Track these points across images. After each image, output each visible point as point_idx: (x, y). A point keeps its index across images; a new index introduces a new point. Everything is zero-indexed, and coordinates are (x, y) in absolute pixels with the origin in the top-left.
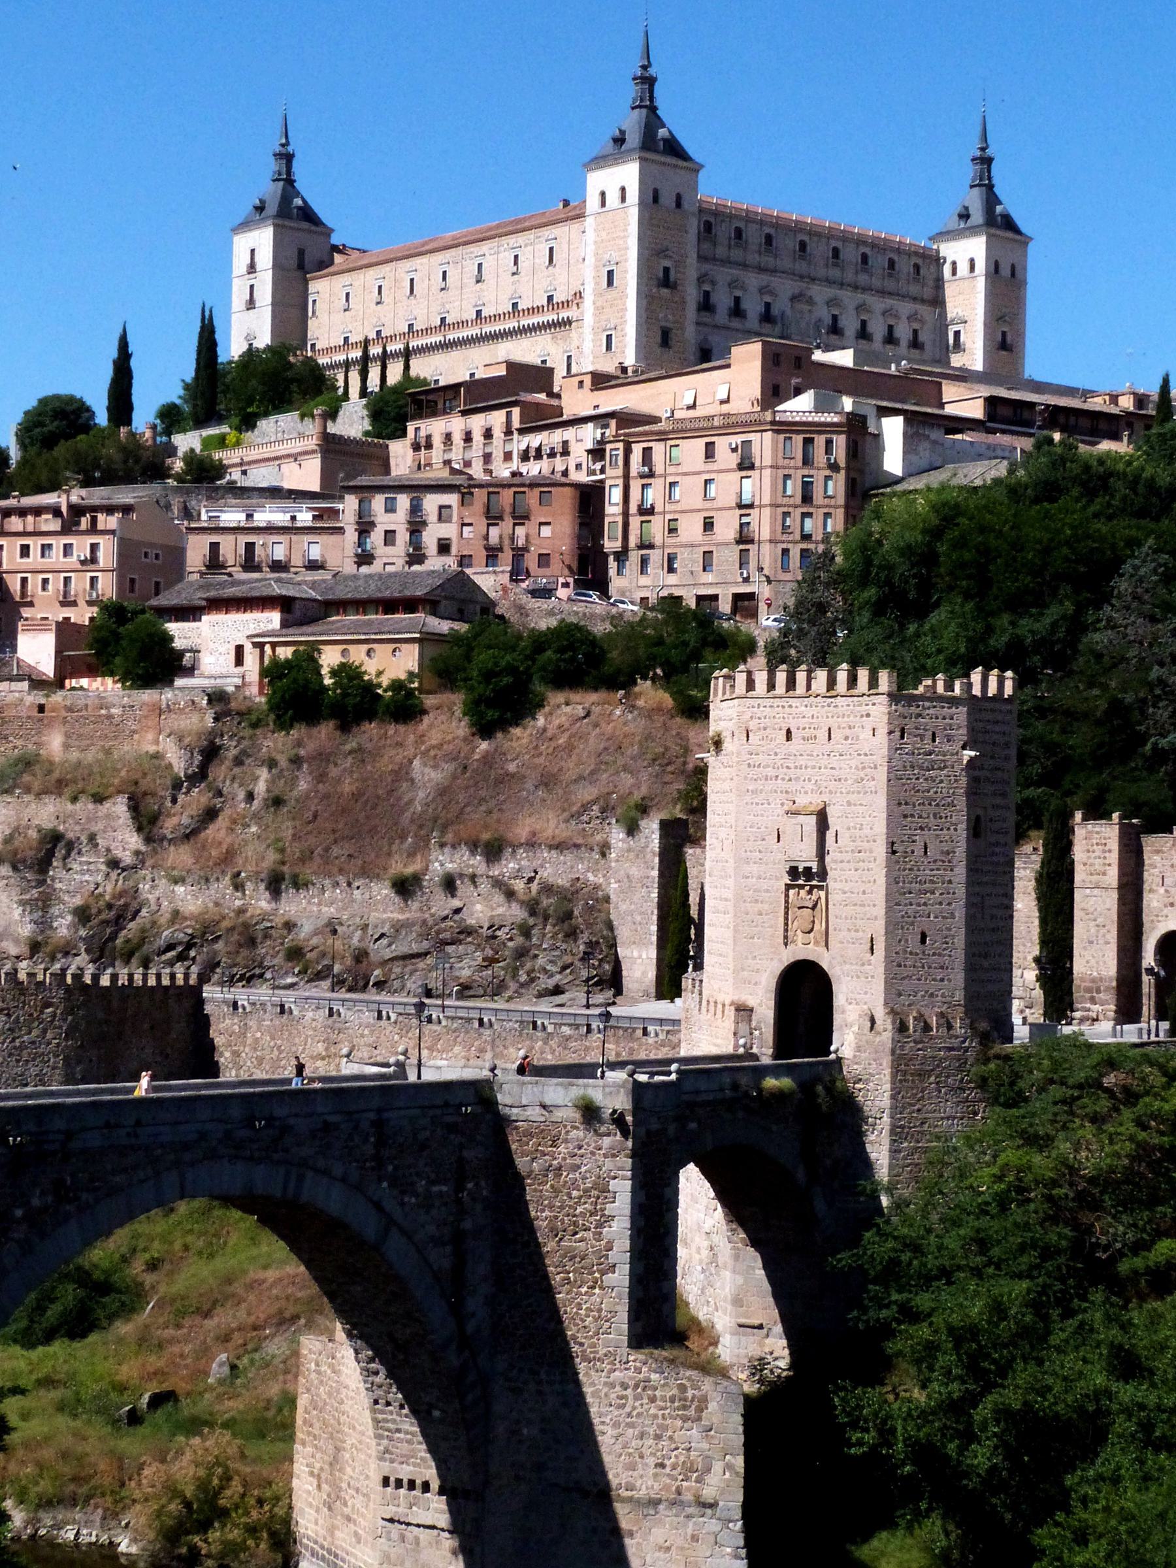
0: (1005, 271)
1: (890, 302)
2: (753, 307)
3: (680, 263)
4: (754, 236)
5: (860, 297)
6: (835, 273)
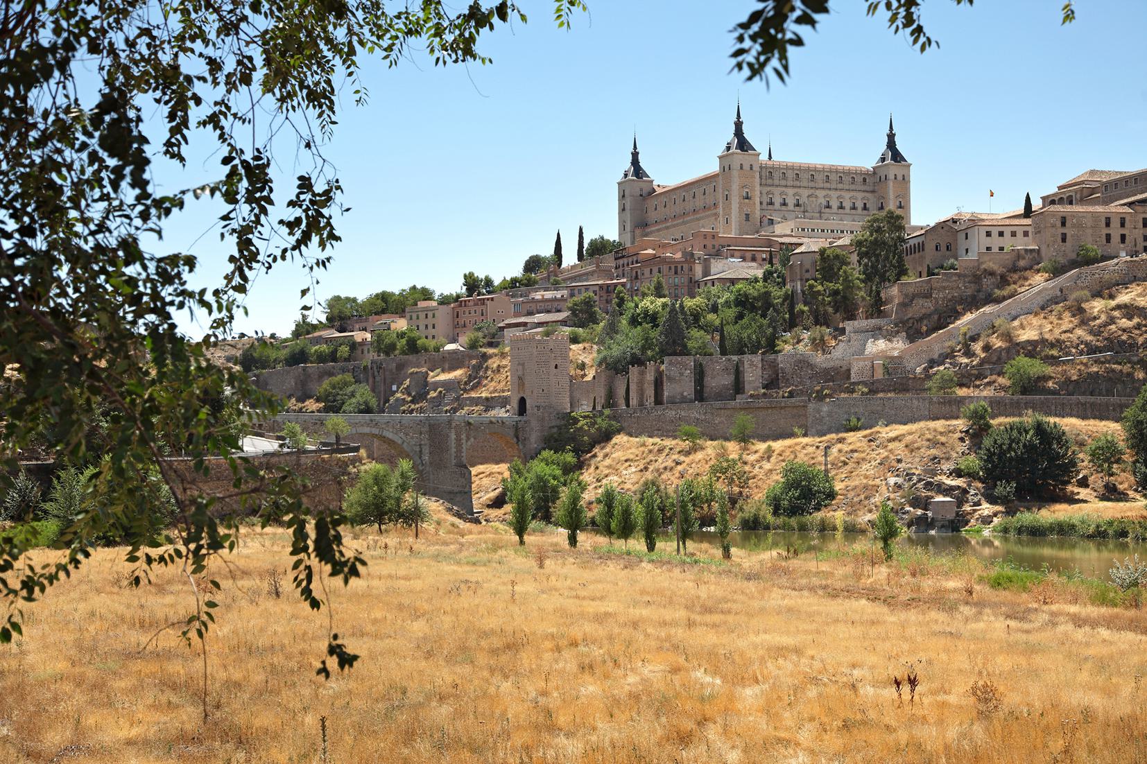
0: (900, 178)
1: (852, 194)
2: (791, 202)
3: (753, 190)
4: (790, 174)
5: (838, 193)
6: (828, 185)
